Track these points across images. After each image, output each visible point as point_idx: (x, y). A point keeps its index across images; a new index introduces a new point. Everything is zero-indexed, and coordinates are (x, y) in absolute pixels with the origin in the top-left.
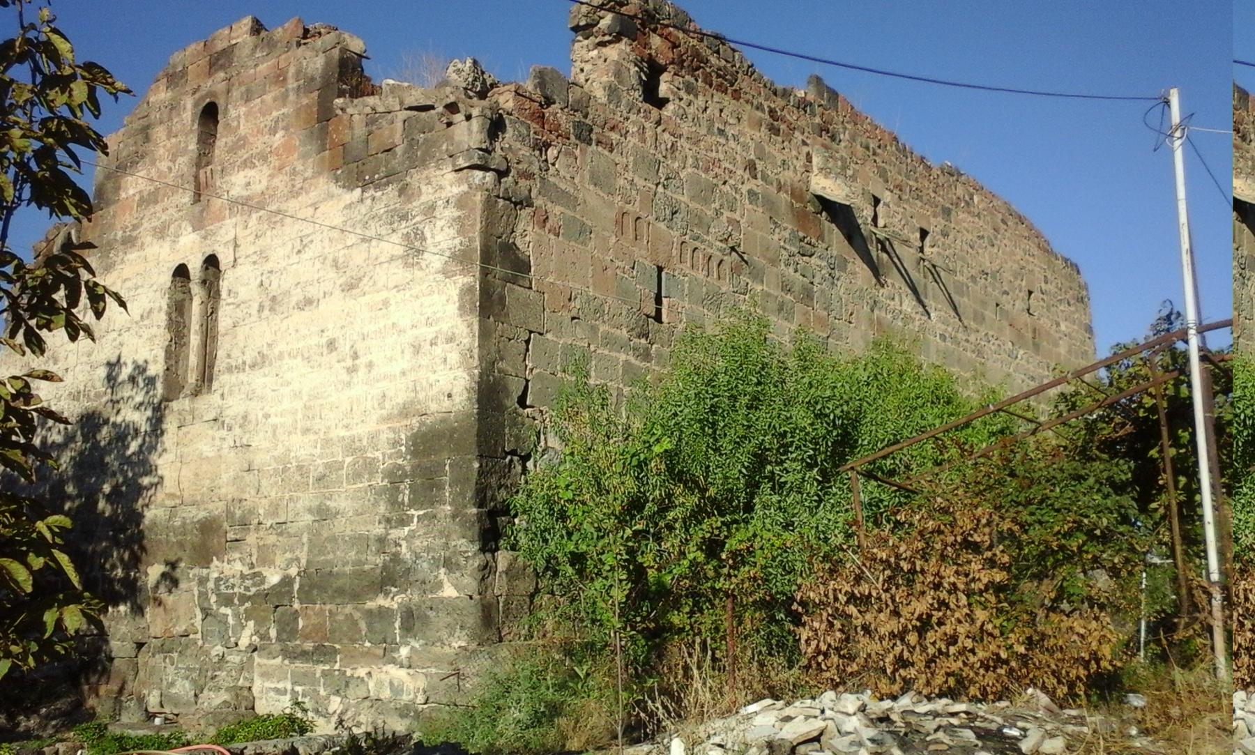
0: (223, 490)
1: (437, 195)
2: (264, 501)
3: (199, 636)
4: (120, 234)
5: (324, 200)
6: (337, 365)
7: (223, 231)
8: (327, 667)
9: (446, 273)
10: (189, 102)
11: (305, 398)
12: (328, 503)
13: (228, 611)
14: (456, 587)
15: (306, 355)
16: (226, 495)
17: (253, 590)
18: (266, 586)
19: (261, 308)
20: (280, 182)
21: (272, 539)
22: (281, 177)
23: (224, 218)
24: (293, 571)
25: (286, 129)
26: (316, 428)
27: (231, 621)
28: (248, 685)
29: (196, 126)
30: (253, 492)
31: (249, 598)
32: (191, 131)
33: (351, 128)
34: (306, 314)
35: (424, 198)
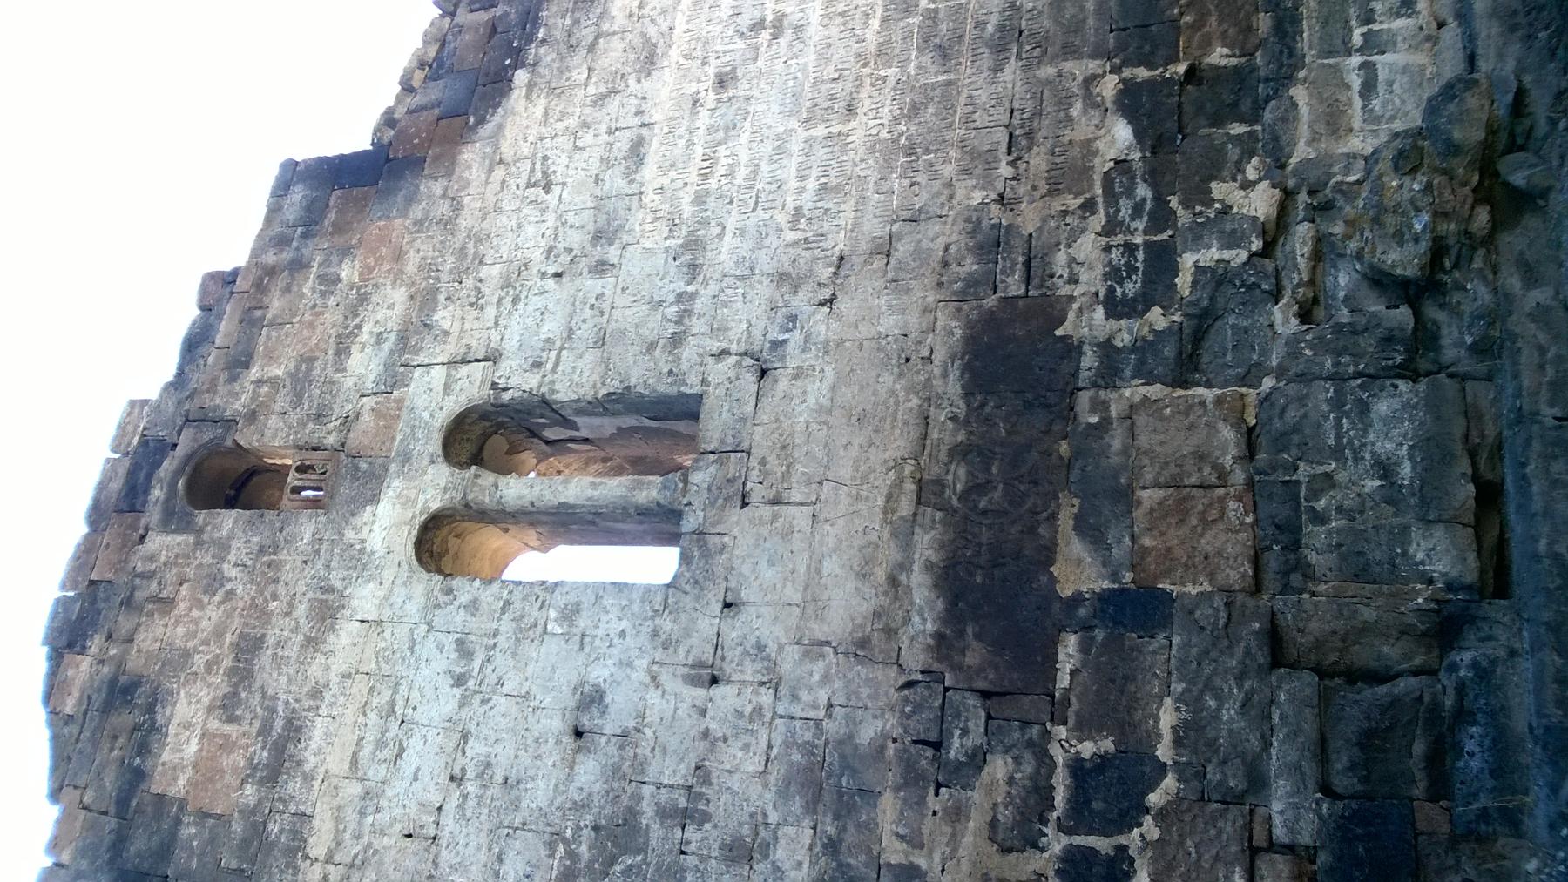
0: (914, 321)
2: (960, 193)
3: (1252, 394)
5: (496, 147)
6: (760, 63)
7: (420, 402)
11: (793, 123)
12: (990, 28)
13: (1188, 260)
15: (721, 134)
16: (926, 310)
17: (1143, 191)
18: (1136, 155)
19: (601, 268)
21: (1038, 161)
22: (412, 252)
23: (400, 401)
24: (1109, 87)
25: (346, 251)
26: (849, 86)
27: (1212, 254)
28: (1361, 164)
29: (201, 516)
30: (935, 227)
31: (1160, 200)
34: (654, 151)
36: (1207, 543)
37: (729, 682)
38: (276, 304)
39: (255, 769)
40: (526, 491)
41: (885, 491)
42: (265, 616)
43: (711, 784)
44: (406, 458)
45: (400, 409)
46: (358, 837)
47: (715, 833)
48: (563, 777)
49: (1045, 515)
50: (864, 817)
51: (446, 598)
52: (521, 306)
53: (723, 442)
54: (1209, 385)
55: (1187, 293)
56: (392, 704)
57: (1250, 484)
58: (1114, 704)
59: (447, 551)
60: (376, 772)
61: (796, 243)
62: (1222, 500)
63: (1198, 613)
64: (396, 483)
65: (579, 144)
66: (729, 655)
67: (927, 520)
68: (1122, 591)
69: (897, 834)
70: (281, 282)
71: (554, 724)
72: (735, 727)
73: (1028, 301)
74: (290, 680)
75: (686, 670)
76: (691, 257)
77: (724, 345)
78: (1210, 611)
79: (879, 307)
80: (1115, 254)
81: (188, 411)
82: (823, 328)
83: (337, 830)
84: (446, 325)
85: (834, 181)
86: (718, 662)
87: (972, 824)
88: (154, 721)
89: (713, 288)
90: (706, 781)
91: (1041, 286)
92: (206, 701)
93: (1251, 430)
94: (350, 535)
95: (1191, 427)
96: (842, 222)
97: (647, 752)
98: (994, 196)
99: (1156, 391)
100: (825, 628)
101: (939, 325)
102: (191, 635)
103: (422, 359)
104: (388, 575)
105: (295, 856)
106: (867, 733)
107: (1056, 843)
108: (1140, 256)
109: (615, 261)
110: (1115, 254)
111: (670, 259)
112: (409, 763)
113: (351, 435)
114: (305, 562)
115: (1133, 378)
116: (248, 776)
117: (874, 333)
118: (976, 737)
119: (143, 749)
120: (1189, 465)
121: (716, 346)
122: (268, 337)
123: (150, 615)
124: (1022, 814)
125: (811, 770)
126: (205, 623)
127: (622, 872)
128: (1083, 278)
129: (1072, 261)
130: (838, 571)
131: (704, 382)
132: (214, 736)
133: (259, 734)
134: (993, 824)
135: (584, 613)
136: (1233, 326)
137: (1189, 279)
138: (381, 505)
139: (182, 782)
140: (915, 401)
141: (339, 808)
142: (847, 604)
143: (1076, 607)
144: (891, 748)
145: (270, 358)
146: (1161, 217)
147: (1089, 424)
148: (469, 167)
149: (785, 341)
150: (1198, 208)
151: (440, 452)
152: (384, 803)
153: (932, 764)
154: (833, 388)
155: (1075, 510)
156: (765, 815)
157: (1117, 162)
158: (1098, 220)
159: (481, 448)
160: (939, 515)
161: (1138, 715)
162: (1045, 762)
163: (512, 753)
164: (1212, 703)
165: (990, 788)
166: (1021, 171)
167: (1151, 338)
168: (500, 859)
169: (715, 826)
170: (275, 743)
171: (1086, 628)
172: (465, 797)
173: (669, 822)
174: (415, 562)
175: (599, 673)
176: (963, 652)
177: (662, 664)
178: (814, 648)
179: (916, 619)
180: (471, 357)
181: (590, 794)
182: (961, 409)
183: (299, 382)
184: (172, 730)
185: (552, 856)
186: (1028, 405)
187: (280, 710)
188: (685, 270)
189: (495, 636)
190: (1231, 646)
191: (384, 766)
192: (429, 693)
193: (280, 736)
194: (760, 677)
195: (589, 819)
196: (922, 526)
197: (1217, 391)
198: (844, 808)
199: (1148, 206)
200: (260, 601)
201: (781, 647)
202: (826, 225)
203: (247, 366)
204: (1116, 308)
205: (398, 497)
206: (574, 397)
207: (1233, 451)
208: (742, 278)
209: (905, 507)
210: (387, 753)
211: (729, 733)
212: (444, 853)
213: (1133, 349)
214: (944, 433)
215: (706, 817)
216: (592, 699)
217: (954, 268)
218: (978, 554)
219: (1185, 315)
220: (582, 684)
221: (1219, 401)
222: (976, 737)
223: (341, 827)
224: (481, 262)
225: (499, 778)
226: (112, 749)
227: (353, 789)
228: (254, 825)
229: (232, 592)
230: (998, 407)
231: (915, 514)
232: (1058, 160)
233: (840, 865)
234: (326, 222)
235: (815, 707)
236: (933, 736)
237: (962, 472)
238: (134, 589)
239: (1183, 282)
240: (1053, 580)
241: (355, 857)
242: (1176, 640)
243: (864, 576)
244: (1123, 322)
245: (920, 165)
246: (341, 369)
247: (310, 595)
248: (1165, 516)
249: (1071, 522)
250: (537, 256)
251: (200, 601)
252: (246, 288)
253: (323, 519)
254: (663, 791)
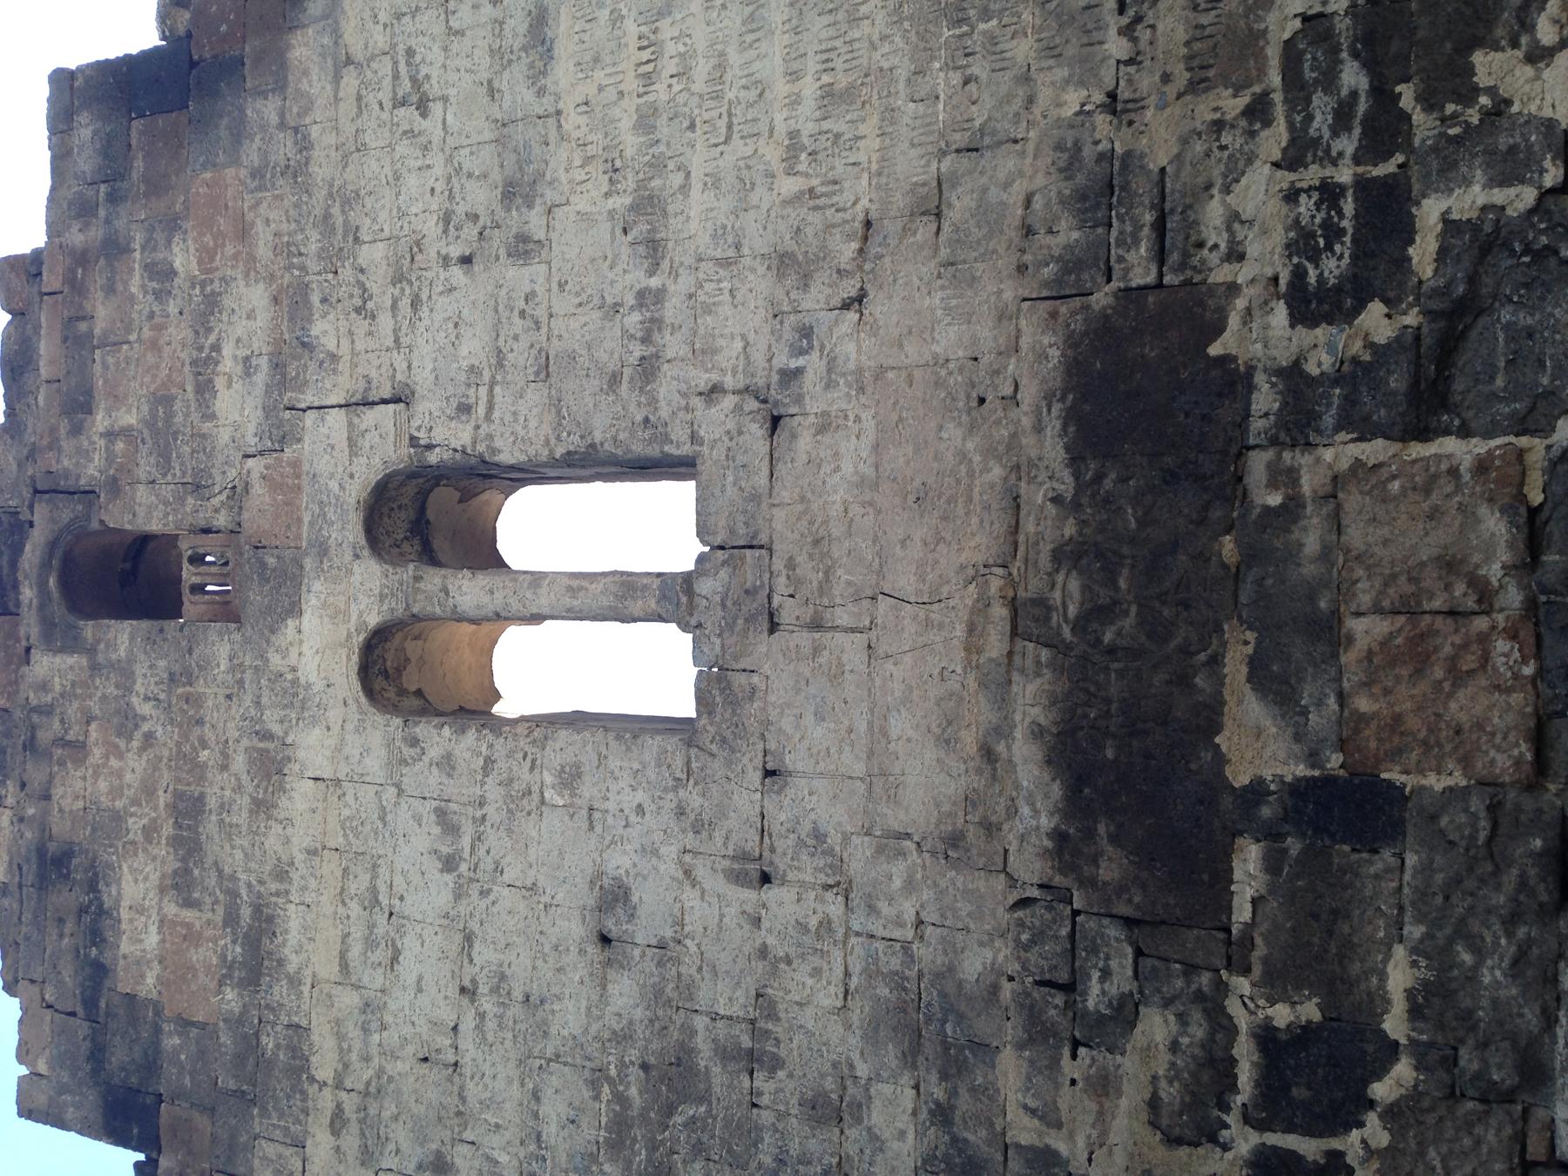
0: (987, 334)
2: (1044, 96)
3: (1536, 449)
4: (231, 998)
5: (337, 34)
7: (323, 465)
13: (1430, 211)
16: (1002, 316)
17: (1353, 77)
19: (524, 248)
20: (270, 220)
22: (259, 226)
23: (296, 464)
25: (172, 225)
27: (1471, 197)
29: (88, 629)
30: (1006, 163)
31: (1383, 95)
32: (91, 651)
34: (564, 28)
36: (1462, 706)
37: (783, 882)
38: (102, 313)
39: (230, 968)
40: (486, 599)
41: (964, 615)
42: (198, 770)
43: (778, 1019)
44: (323, 551)
45: (298, 477)
46: (367, 1059)
47: (791, 1085)
48: (595, 997)
49: (1202, 657)
50: (980, 1080)
51: (413, 752)
52: (424, 312)
53: (732, 532)
54: (1465, 432)
55: (1429, 273)
56: (374, 890)
57: (1531, 605)
58: (1317, 946)
59: (408, 660)
60: (374, 979)
61: (795, 200)
62: (1484, 639)
63: (1444, 821)
64: (317, 586)
65: (455, 24)
66: (780, 845)
67: (1029, 662)
68: (1328, 781)
69: (1025, 1107)
70: (99, 278)
71: (573, 928)
72: (799, 945)
73: (1163, 294)
74: (246, 855)
75: (726, 863)
76: (646, 224)
77: (715, 377)
78: (1463, 818)
79: (933, 310)
80: (1306, 205)
81: (33, 478)
82: (851, 348)
83: (341, 1050)
84: (331, 344)
85: (843, 81)
86: (766, 854)
87: (1124, 1102)
88: (101, 906)
89: (685, 282)
90: (772, 1016)
91: (1182, 266)
92: (155, 878)
93: (1534, 512)
94: (275, 660)
95: (1434, 514)
96: (862, 158)
97: (693, 971)
98: (1099, 97)
99: (1376, 450)
100: (902, 815)
101: (1025, 342)
102: (117, 792)
103: (309, 398)
104: (334, 715)
105: (300, 1078)
106: (973, 965)
107: (1245, 1141)
108: (1349, 206)
109: (540, 234)
110: (1306, 205)
111: (618, 231)
112: (409, 968)
113: (245, 515)
114: (229, 697)
115: (1338, 429)
116: (224, 976)
117: (928, 357)
118: (1122, 979)
119: (96, 936)
120: (1430, 579)
121: (703, 379)
122: (105, 366)
123: (62, 763)
124: (1193, 1094)
125: (904, 1011)
126: (128, 777)
127: (685, 1125)
128: (1253, 250)
129: (1234, 217)
130: (910, 733)
131: (694, 438)
132: (174, 924)
133: (226, 924)
134: (1154, 1103)
135: (587, 778)
136: (1508, 327)
137: (1432, 246)
138: (306, 617)
139: (150, 980)
140: (997, 472)
141: (338, 1022)
142: (928, 784)
143: (1257, 804)
144: (1007, 989)
145: (117, 400)
146: (1384, 130)
147: (1267, 510)
148: (306, 73)
149: (799, 372)
150: (1450, 108)
151: (363, 542)
152: (388, 1018)
153: (1066, 1020)
154: (876, 447)
155: (1250, 650)
156: (852, 1066)
157: (1306, 19)
158: (1274, 139)
159: (422, 510)
160: (1045, 654)
161: (1355, 969)
162: (1222, 1026)
163: (528, 962)
164: (1467, 958)
165: (1147, 1052)
166: (1143, 45)
167: (1367, 357)
168: (537, 1098)
169: (790, 1076)
170: (246, 936)
171: (1271, 834)
172: (482, 1016)
173: (732, 1066)
174: (363, 699)
175: (620, 862)
176: (1095, 862)
177: (696, 854)
178: (892, 841)
179: (1025, 810)
180: (374, 396)
181: (631, 1023)
182: (1067, 486)
183: (161, 433)
184: (124, 914)
185: (597, 1098)
186: (1171, 477)
187: (244, 893)
188: (641, 249)
189: (481, 805)
190: (1497, 871)
191: (380, 971)
192: (416, 879)
193: (250, 927)
194: (822, 878)
195: (633, 1055)
196: (1022, 671)
197: (1479, 446)
198: (953, 1065)
199: (1362, 107)
200: (187, 748)
201: (846, 838)
202: (839, 165)
203: (88, 409)
204: (1309, 305)
205: (324, 605)
206: (523, 458)
207: (1504, 556)
208: (725, 263)
209: (995, 644)
210: (382, 955)
211: (792, 951)
212: (470, 1085)
213: (1338, 378)
214: (1046, 527)
215: (776, 1064)
216: (614, 896)
217: (1042, 239)
218: (1107, 714)
219: (1426, 313)
220: (600, 874)
221: (1482, 466)
223: (345, 1046)
224: (356, 239)
225: (518, 994)
226: (61, 936)
227: (348, 1000)
228: (245, 1037)
229: (149, 737)
230: (1123, 480)
231: (1010, 654)
232: (1205, 19)
233: (955, 1140)
234: (135, 176)
235: (902, 925)
236: (1063, 976)
237: (1074, 585)
238: (33, 728)
239: (1423, 254)
240: (1220, 759)
241: (368, 1083)
242: (1411, 859)
243: (947, 742)
244: (1319, 331)
245: (976, 42)
246: (213, 416)
247: (245, 742)
248: (1393, 662)
249: (1244, 670)
250: (431, 227)
251: (117, 747)
252: (57, 286)
253: (237, 637)
254: (720, 1024)
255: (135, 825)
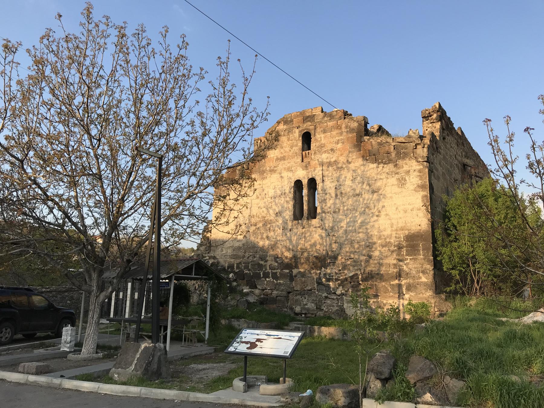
1: (410, 168)
4: (268, 169)
8: (375, 300)
9: (415, 190)
10: (297, 131)
14: (426, 278)
25: (343, 143)
29: (301, 138)
33: (372, 146)
35: (404, 169)
36: (299, 286)
58: (283, 276)
94: (298, 168)
107: (270, 271)
118: (279, 262)
145: (325, 137)
204: (325, 274)
222: (279, 262)
255: (282, 150)
